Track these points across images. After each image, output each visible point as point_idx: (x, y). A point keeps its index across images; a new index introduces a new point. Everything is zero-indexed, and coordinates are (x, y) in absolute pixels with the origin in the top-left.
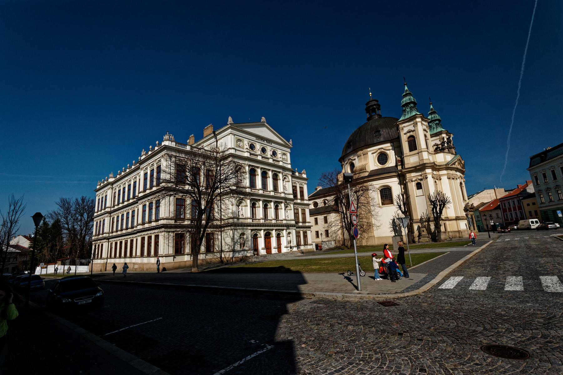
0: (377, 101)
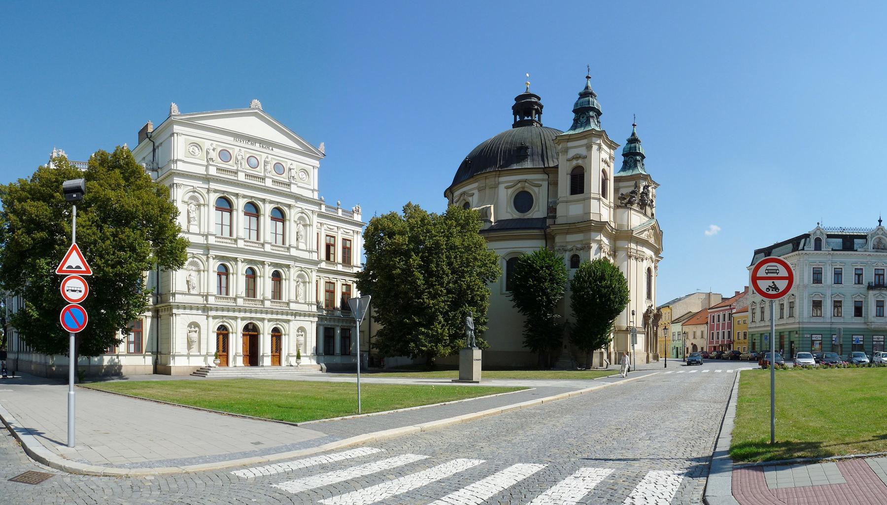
0: (539, 99)
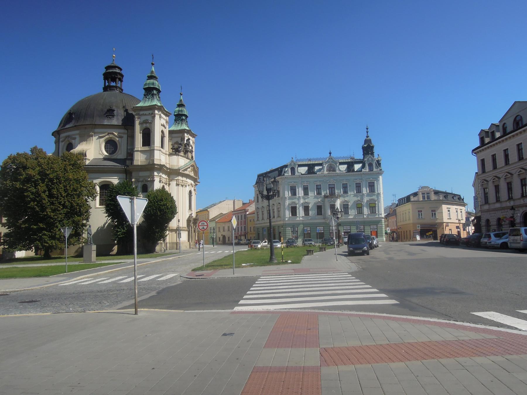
0: (121, 69)
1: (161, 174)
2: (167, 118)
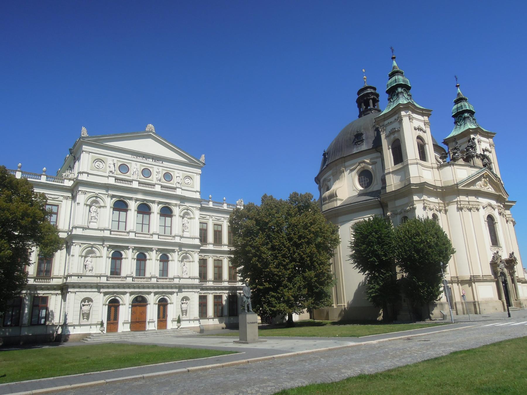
0: (374, 89)
1: (425, 197)
2: (491, 140)
